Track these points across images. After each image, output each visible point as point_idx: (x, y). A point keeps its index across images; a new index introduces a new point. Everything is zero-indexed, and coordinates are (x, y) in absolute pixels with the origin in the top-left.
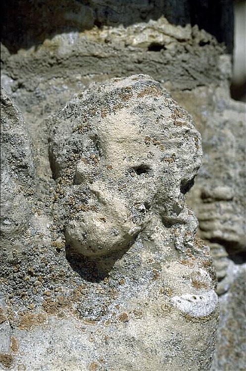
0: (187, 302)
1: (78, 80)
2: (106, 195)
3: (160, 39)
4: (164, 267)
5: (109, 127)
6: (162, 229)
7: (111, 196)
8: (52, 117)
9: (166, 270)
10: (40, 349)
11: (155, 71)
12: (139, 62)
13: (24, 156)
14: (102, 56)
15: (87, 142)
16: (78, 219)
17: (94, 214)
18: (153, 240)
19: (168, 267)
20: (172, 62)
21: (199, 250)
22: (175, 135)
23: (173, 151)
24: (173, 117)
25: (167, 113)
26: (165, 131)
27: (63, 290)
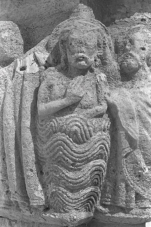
1: (121, 28)
2: (134, 54)
3: (144, 18)
10: (117, 94)
15: (128, 41)
16: (126, 61)
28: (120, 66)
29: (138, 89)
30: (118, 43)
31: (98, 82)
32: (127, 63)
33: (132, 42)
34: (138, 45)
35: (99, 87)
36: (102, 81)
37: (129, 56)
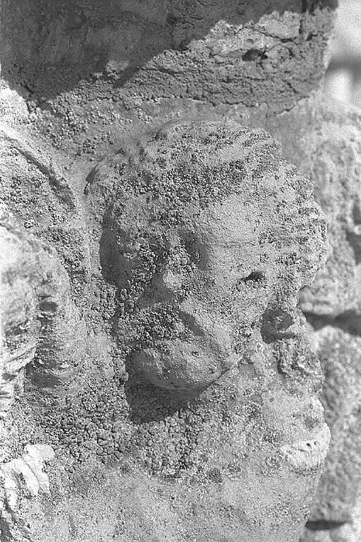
0: (299, 452)
1: (137, 107)
2: (204, 320)
3: (260, 45)
4: (266, 400)
5: (212, 224)
6: (263, 345)
7: (212, 323)
8: (112, 184)
9: (270, 404)
11: (249, 92)
12: (229, 81)
13: (82, 258)
14: (176, 71)
15: (175, 241)
16: (159, 347)
17: (185, 345)
18: (252, 363)
19: (272, 400)
20: (272, 75)
21: (311, 372)
22: (300, 227)
23: (294, 248)
24: (299, 202)
25: (291, 196)
26: (286, 223)
27: (123, 429)
28: (130, 360)
29: (213, 487)
30: (120, 231)
31: (7, 508)
32: (166, 362)
33: (196, 248)
34: (226, 267)
35: (12, 532)
36: (29, 497)
37: (180, 327)
